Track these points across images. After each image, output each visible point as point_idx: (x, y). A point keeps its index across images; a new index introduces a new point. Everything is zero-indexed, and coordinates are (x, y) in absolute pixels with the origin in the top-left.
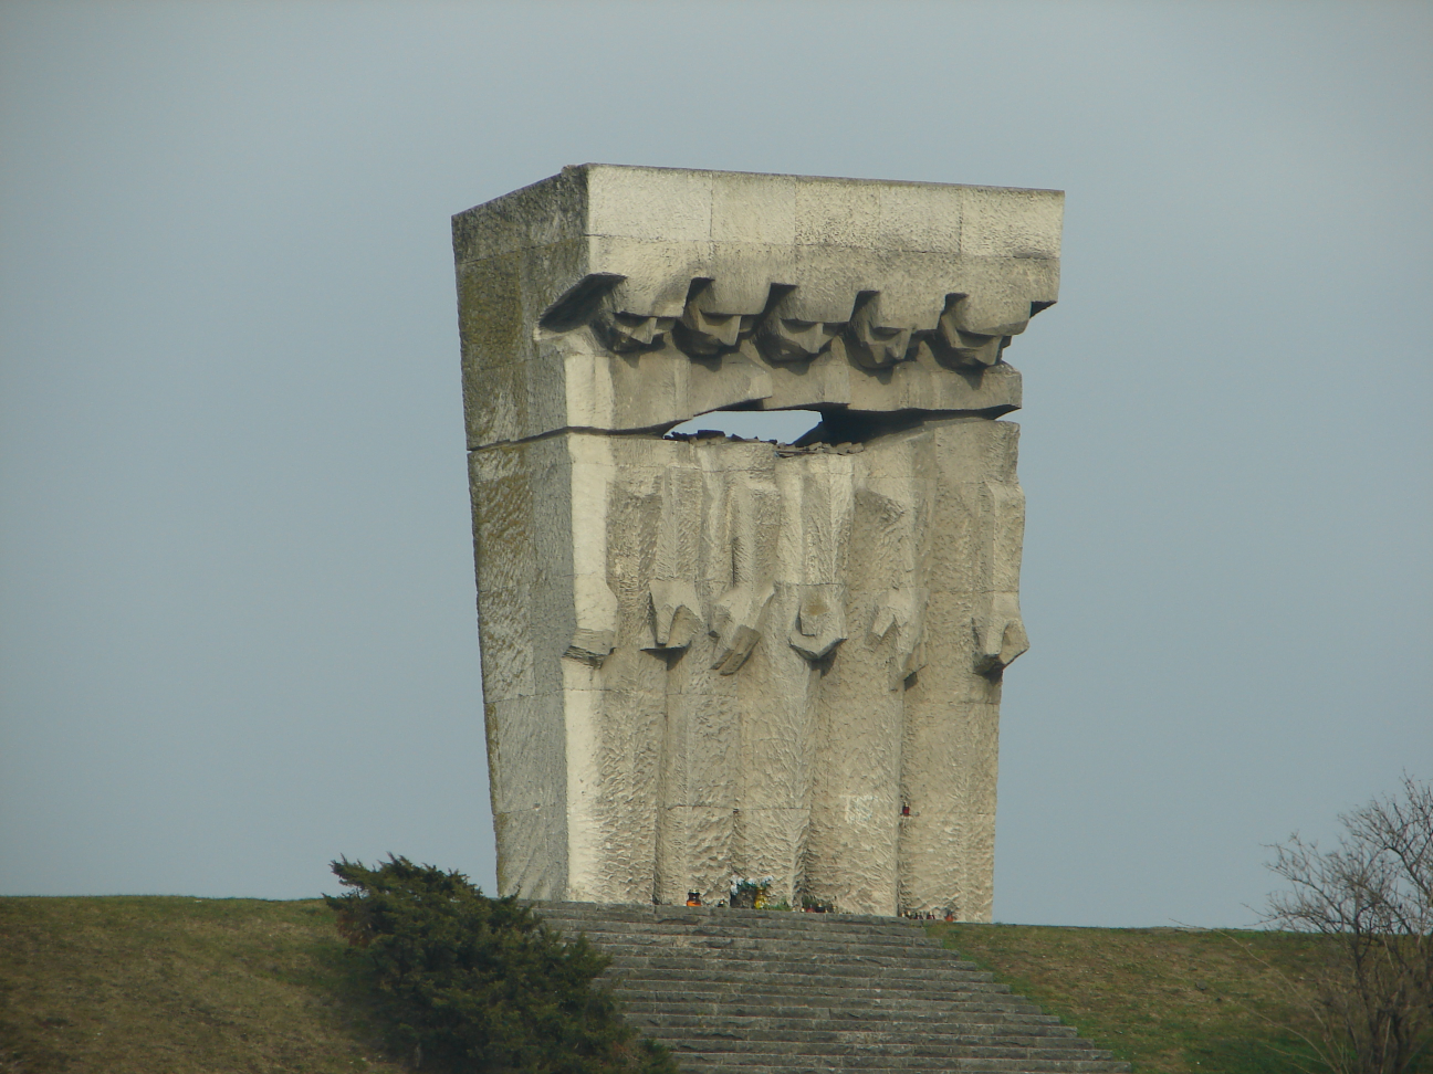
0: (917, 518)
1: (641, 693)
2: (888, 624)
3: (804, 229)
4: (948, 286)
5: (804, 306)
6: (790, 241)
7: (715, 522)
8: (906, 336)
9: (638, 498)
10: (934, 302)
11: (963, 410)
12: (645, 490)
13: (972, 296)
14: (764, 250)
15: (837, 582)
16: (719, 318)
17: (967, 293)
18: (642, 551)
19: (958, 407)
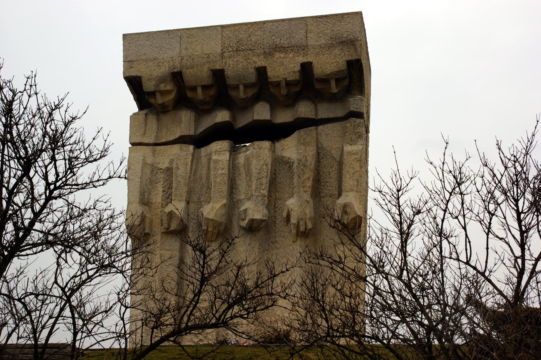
0: (299, 163)
1: (163, 252)
2: (286, 211)
3: (226, 46)
4: (302, 59)
5: (228, 78)
6: (219, 51)
7: (205, 176)
8: (283, 84)
9: (161, 169)
10: (294, 67)
11: (334, 118)
12: (166, 165)
13: (314, 62)
14: (205, 56)
15: (257, 194)
16: (194, 89)
17: (311, 61)
18: (163, 191)
19: (331, 116)
